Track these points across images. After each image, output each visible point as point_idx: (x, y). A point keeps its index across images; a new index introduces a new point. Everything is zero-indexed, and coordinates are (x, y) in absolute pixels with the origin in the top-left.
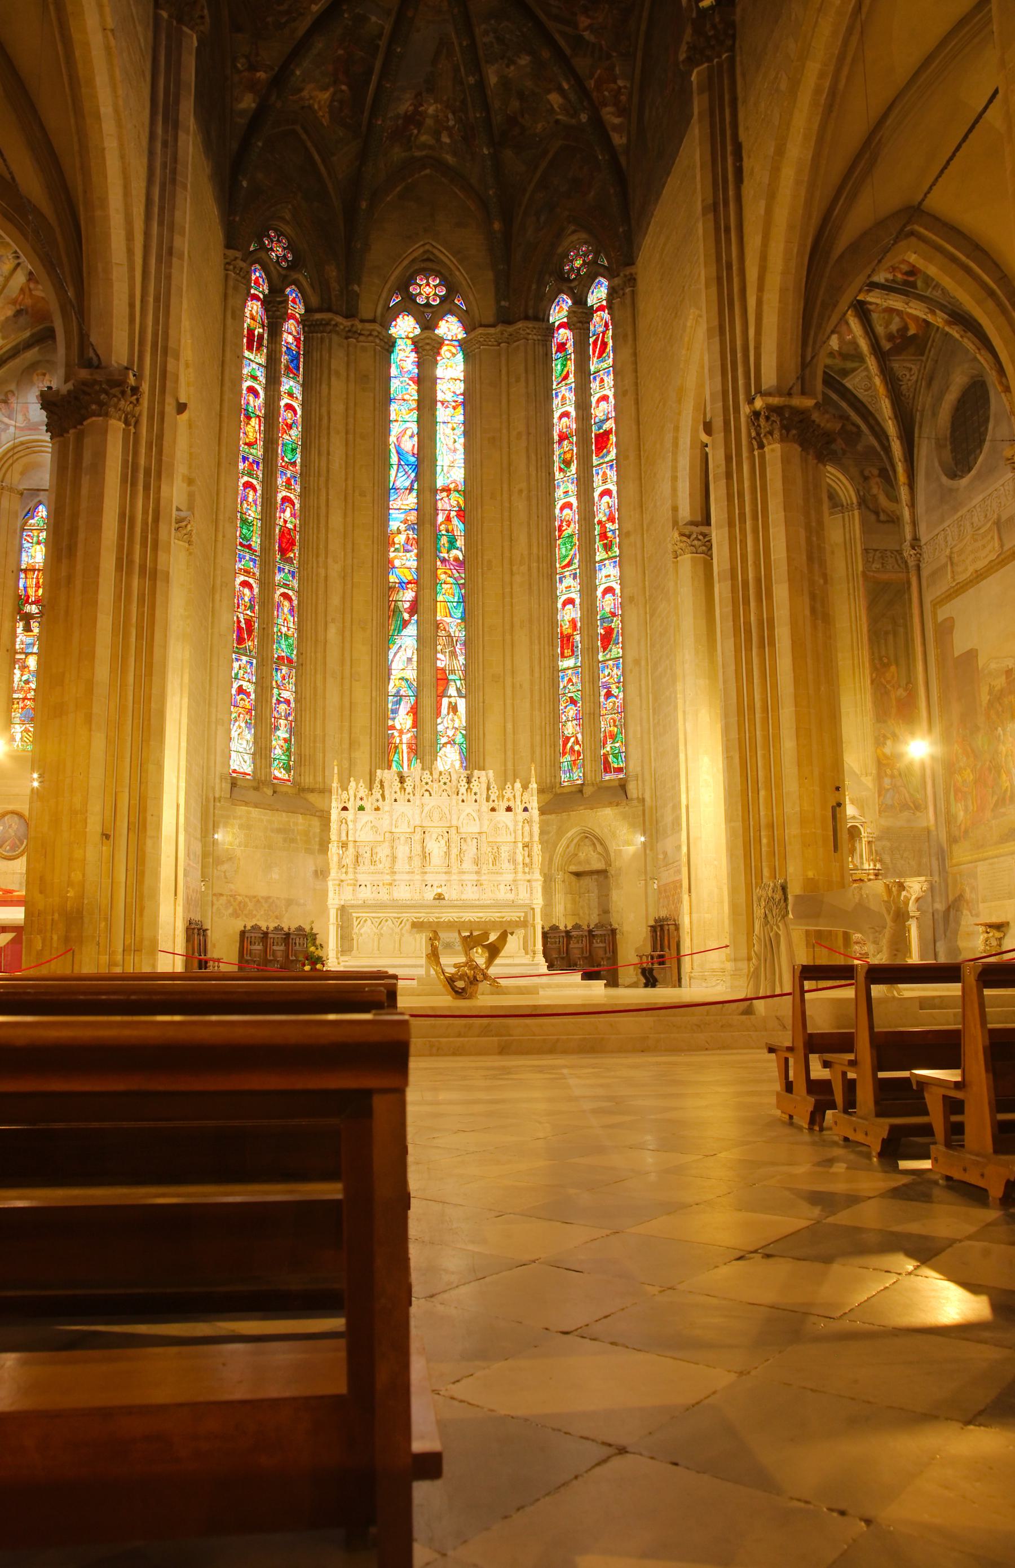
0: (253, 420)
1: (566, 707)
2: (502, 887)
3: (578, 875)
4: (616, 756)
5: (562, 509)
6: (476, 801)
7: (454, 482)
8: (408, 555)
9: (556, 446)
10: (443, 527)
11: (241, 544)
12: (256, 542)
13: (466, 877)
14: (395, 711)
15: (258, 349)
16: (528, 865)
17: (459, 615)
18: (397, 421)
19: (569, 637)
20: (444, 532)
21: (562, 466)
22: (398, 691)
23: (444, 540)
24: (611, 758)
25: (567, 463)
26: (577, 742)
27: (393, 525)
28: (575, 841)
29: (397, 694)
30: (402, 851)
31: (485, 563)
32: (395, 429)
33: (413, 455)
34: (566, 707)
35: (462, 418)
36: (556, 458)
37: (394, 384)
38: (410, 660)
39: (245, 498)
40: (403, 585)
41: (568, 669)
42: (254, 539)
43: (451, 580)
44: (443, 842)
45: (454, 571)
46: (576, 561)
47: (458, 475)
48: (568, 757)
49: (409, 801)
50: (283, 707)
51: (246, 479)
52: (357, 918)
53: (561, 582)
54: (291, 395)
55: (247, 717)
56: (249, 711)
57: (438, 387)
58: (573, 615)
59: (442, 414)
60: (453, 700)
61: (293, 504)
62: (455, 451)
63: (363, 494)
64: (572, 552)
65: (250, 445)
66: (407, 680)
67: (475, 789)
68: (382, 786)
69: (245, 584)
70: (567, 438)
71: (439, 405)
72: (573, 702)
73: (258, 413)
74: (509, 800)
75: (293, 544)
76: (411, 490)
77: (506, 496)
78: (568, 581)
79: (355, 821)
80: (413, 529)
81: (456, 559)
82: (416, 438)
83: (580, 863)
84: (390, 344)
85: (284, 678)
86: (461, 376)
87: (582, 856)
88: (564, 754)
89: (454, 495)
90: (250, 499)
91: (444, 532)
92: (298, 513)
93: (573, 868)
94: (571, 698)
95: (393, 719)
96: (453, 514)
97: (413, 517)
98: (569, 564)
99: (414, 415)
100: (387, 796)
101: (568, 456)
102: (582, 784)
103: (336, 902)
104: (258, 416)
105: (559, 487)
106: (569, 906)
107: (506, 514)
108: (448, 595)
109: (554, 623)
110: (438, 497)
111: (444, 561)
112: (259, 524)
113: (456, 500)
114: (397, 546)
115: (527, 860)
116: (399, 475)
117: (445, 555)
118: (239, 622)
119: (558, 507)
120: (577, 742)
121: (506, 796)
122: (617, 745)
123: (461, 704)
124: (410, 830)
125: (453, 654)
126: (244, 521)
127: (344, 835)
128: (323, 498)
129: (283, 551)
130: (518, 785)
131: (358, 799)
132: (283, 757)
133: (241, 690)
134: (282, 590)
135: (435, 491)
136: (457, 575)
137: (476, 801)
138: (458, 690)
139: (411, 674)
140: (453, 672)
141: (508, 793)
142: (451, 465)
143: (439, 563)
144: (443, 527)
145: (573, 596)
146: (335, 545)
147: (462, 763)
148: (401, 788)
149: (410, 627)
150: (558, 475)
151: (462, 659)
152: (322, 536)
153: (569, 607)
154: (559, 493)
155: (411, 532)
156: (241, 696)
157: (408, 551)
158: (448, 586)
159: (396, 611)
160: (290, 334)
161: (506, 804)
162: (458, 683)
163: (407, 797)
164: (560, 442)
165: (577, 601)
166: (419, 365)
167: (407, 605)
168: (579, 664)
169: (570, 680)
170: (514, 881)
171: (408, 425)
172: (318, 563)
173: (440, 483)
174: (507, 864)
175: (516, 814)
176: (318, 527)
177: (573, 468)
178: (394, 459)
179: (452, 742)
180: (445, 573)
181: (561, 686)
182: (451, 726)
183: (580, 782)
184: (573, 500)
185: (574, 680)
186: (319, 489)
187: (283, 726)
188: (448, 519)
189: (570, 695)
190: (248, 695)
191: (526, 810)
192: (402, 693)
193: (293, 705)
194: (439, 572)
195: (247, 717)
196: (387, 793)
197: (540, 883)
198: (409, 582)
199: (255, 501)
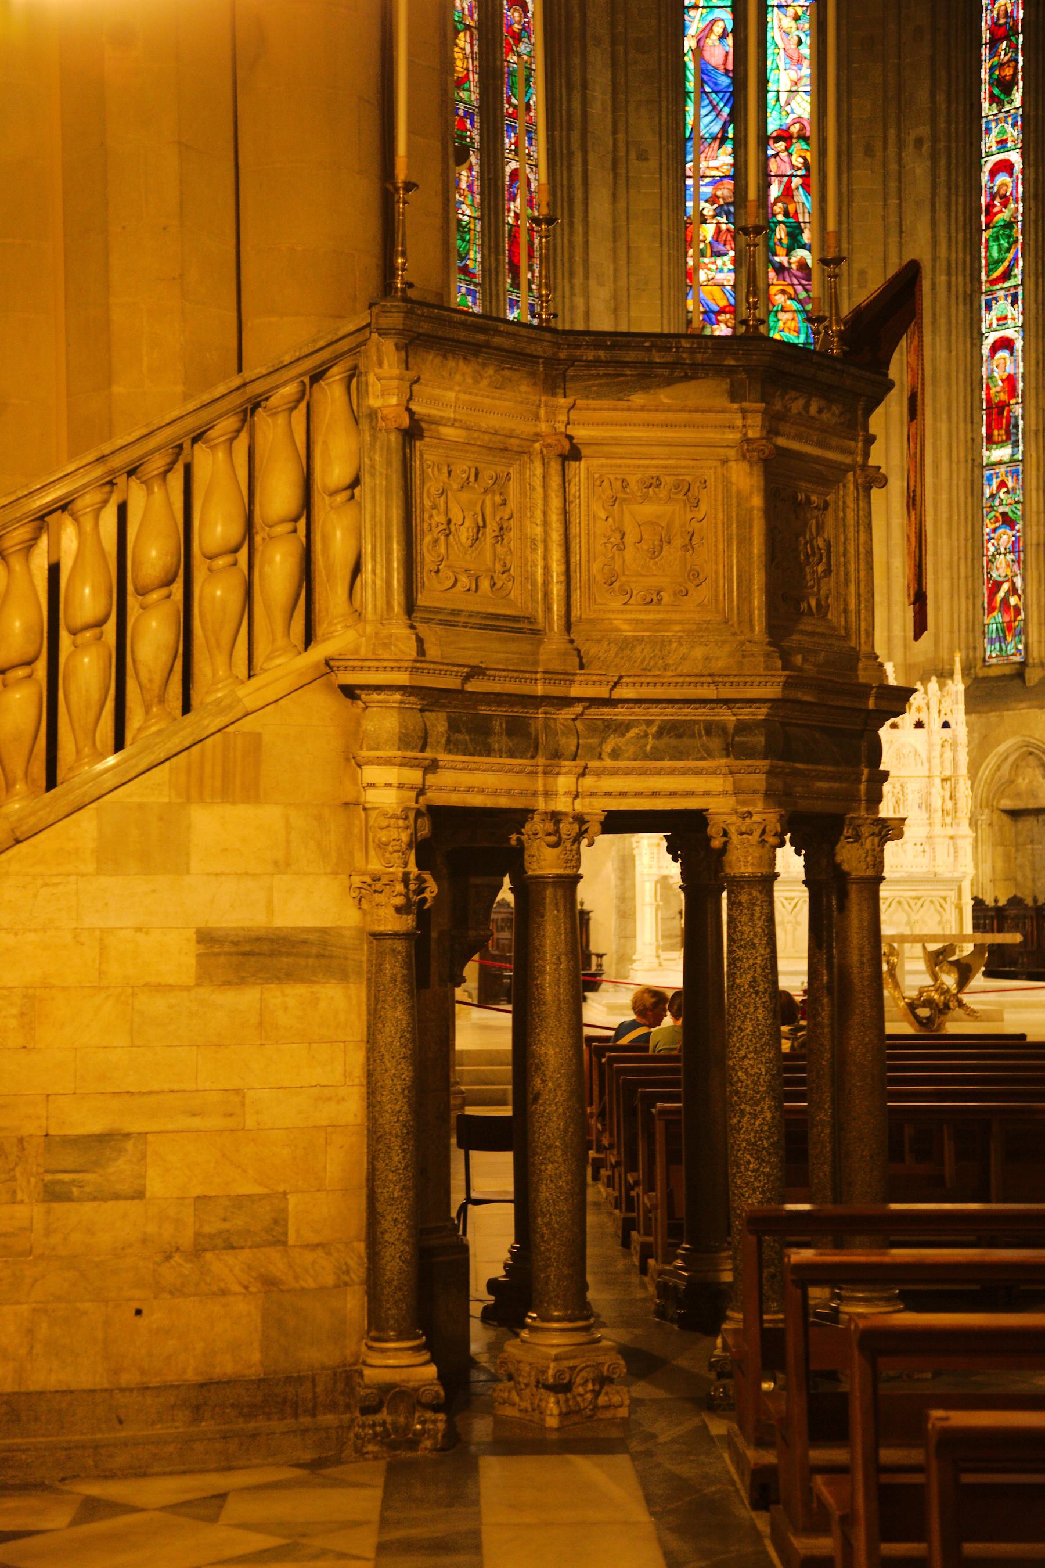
0: (462, 35)
1: (994, 531)
3: (1014, 814)
5: (993, 173)
7: (799, 120)
8: (719, 261)
9: (985, 51)
10: (778, 208)
16: (950, 813)
18: (696, 7)
19: (1002, 406)
20: (780, 217)
21: (996, 91)
23: (781, 233)
25: (1006, 86)
26: (1013, 590)
28: (1011, 759)
31: (855, 276)
32: (694, 23)
33: (727, 71)
34: (994, 531)
36: (984, 75)
41: (1000, 463)
42: (472, 255)
43: (794, 305)
45: (799, 288)
46: (1018, 271)
47: (803, 107)
48: (998, 616)
53: (989, 308)
58: (1010, 369)
62: (799, 61)
63: (642, 157)
64: (1010, 256)
70: (1007, 38)
74: (919, 710)
76: (723, 140)
77: (892, 151)
78: (1002, 307)
80: (728, 214)
81: (803, 265)
82: (730, 41)
83: (1018, 795)
87: (1022, 783)
88: (992, 609)
89: (798, 146)
90: (464, 185)
91: (780, 217)
93: (1007, 804)
94: (1004, 515)
96: (796, 182)
98: (1007, 275)
101: (1008, 72)
102: (1021, 663)
103: (654, 871)
104: (468, 27)
105: (988, 131)
106: (1000, 865)
107: (893, 185)
109: (974, 382)
110: (770, 152)
111: (780, 269)
112: (478, 228)
115: (949, 805)
116: (703, 112)
117: (781, 259)
119: (987, 169)
120: (1013, 590)
128: (578, 169)
135: (764, 140)
136: (803, 295)
143: (772, 274)
144: (778, 208)
145: (1010, 333)
146: (600, 254)
150: (987, 109)
152: (578, 239)
153: (1003, 354)
154: (989, 142)
155: (724, 220)
157: (719, 254)
158: (788, 316)
164: (994, 43)
165: (1019, 345)
168: (1019, 456)
169: (1002, 484)
170: (929, 837)
171: (717, 13)
172: (572, 288)
173: (773, 126)
175: (930, 733)
176: (571, 224)
177: (1017, 97)
180: (783, 292)
181: (987, 493)
183: (1018, 659)
184: (1015, 157)
185: (1010, 484)
186: (570, 154)
188: (788, 193)
189: (1001, 509)
191: (946, 725)
194: (773, 290)
197: (970, 840)
198: (722, 311)
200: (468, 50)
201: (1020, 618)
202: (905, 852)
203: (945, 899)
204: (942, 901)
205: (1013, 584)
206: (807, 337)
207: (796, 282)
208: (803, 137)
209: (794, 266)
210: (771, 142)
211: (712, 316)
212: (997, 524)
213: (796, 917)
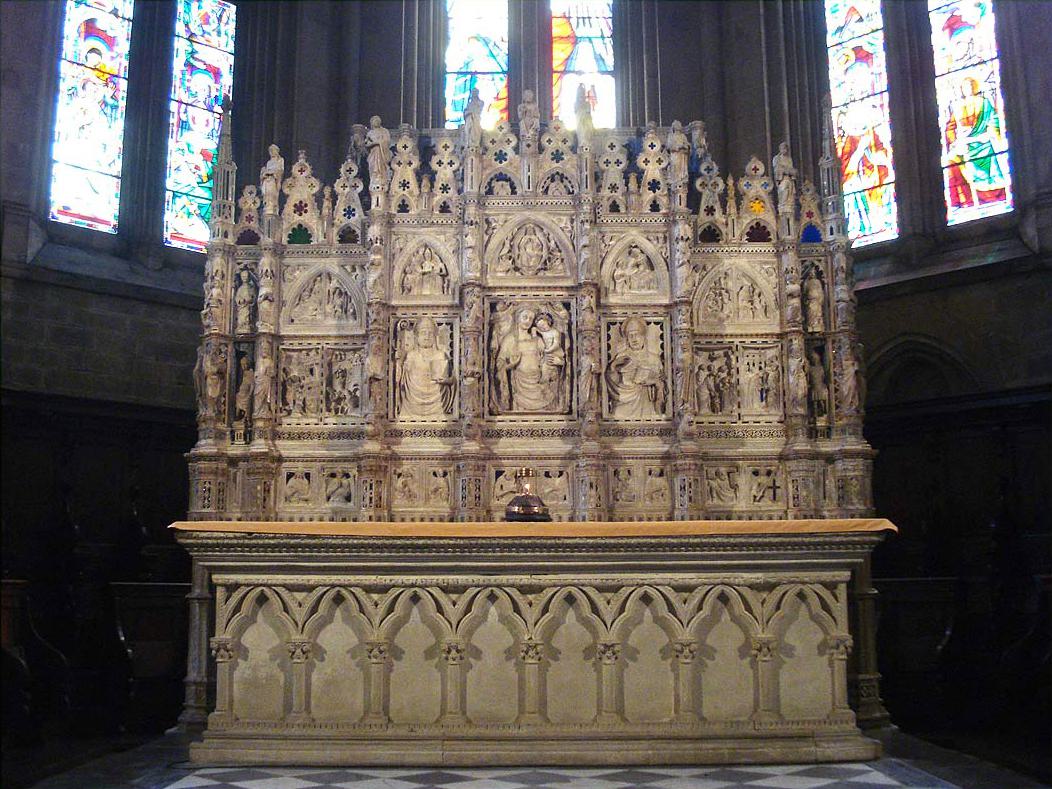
2: (743, 480)
4: (982, 163)
6: (655, 207)
13: (623, 447)
24: (969, 172)
26: (878, 145)
30: (425, 362)
44: (552, 336)
49: (444, 209)
50: (201, 83)
52: (231, 588)
55: (109, 92)
67: (652, 172)
68: (364, 175)
72: (862, 56)
79: (278, 276)
85: (206, 20)
100: (377, 197)
121: (752, 193)
122: (982, 138)
124: (448, 301)
127: (243, 315)
130: (783, 162)
131: (289, 208)
132: (199, 192)
133: (90, 29)
137: (655, 207)
138: (600, 59)
141: (756, 187)
148: (419, 175)
156: (93, 43)
161: (747, 221)
162: (598, 42)
163: (439, 197)
174: (758, 406)
190: (110, 42)
195: (109, 92)
196: (375, 182)
201: (885, 181)
202: (735, 487)
203: (831, 586)
204: (826, 594)
205: (876, 138)
212: (848, 64)
213: (470, 633)
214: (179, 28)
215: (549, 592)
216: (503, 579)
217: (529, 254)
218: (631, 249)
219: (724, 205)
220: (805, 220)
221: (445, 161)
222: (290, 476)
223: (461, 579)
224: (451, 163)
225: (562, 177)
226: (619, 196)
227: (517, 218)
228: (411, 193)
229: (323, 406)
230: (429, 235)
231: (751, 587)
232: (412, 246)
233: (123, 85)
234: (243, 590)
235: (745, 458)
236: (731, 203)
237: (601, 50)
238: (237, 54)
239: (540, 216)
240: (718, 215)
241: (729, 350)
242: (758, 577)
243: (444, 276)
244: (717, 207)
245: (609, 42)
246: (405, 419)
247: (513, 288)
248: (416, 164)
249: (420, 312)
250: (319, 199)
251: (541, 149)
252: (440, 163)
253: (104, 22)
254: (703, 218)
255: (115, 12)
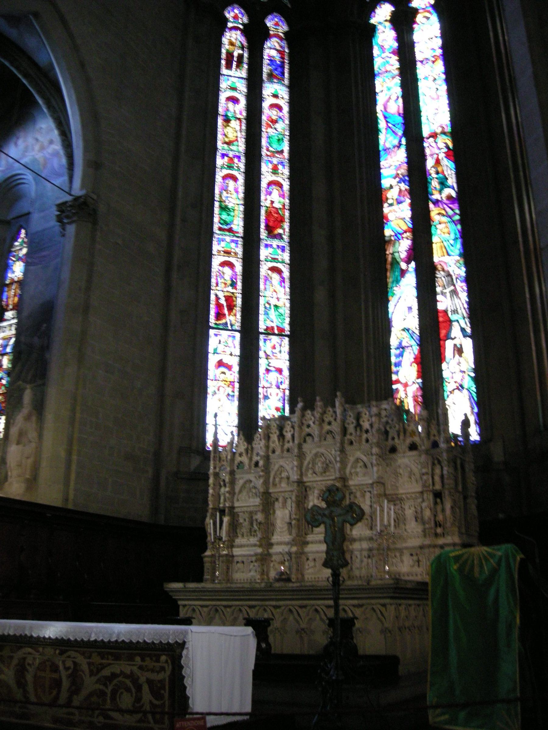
6: (367, 441)
11: (220, 229)
12: (238, 225)
14: (398, 364)
15: (238, 66)
17: (458, 252)
22: (400, 343)
23: (435, 184)
27: (385, 183)
29: (401, 347)
32: (381, 100)
35: (442, 69)
37: (378, 63)
38: (410, 308)
39: (225, 189)
40: (398, 236)
43: (445, 219)
45: (448, 209)
50: (273, 376)
51: (226, 172)
52: (184, 606)
54: (275, 96)
56: (232, 383)
57: (416, 50)
59: (421, 71)
60: (457, 342)
61: (280, 186)
65: (229, 143)
66: (408, 330)
67: (366, 425)
69: (223, 264)
71: (419, 65)
73: (239, 116)
75: (282, 220)
76: (399, 146)
81: (449, 198)
82: (400, 101)
84: (371, 31)
86: (438, 33)
92: (287, 193)
95: (397, 373)
96: (442, 156)
97: (403, 170)
99: (398, 80)
108: (446, 237)
111: (436, 203)
113: (444, 142)
114: (390, 201)
117: (436, 196)
118: (217, 298)
123: (468, 345)
125: (454, 292)
126: (224, 208)
129: (270, 229)
133: (220, 364)
134: (271, 265)
136: (450, 212)
138: (463, 330)
139: (414, 323)
140: (455, 312)
142: (436, 111)
147: (472, 408)
149: (407, 275)
151: (464, 296)
156: (222, 369)
158: (443, 226)
159: (395, 263)
160: (272, 50)
161: (409, 441)
166: (399, 39)
167: (404, 255)
178: (382, 124)
179: (460, 387)
180: (439, 214)
182: (457, 370)
187: (274, 394)
188: (438, 162)
190: (229, 368)
192: (404, 344)
193: (286, 373)
199: (237, 191)
200: (238, 128)
202: (402, 561)
206: (456, 234)
207: (445, 206)
208: (444, 133)
209: (444, 199)
210: (425, 140)
211: (399, 236)
214: (261, 354)
215: (283, 608)
216: (267, 603)
217: (319, 467)
218: (357, 460)
219: (399, 436)
220: (432, 438)
221: (288, 430)
222: (237, 562)
223: (253, 603)
224: (290, 431)
225: (331, 432)
226: (353, 438)
227: (314, 452)
228: (276, 445)
229: (249, 534)
230: (282, 462)
231: (354, 606)
232: (277, 467)
233: (237, 385)
234: (188, 607)
235: (407, 548)
236: (402, 434)
237: (463, 326)
238: (290, 360)
239: (322, 450)
240: (396, 440)
241: (401, 500)
242: (355, 602)
243: (288, 478)
244: (396, 437)
245: (467, 320)
246: (275, 538)
247: (312, 482)
248: (278, 433)
249: (279, 494)
250: (247, 450)
251: (323, 421)
252: (286, 432)
253: (227, 360)
254: (390, 442)
255: (231, 355)
